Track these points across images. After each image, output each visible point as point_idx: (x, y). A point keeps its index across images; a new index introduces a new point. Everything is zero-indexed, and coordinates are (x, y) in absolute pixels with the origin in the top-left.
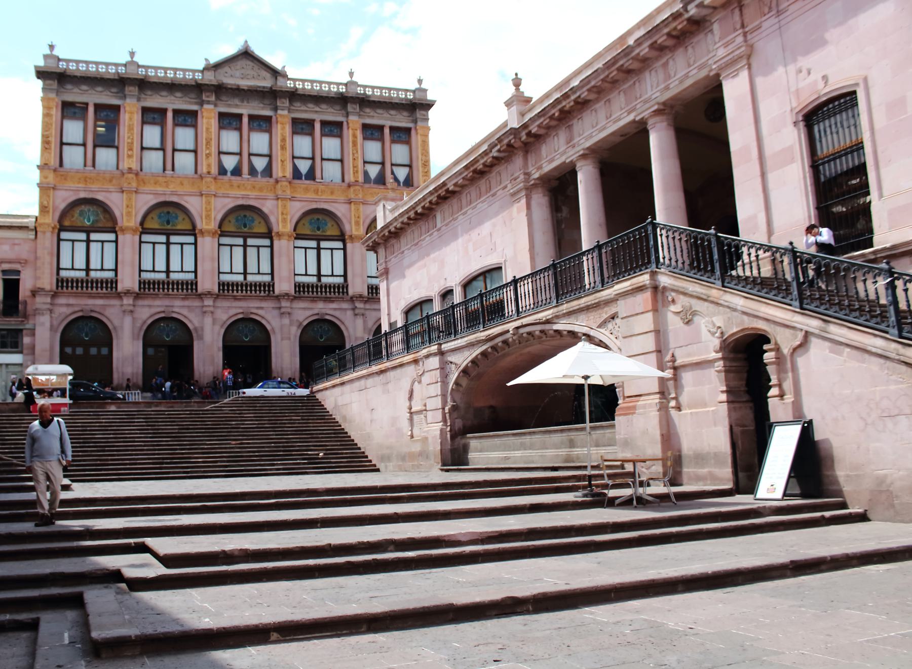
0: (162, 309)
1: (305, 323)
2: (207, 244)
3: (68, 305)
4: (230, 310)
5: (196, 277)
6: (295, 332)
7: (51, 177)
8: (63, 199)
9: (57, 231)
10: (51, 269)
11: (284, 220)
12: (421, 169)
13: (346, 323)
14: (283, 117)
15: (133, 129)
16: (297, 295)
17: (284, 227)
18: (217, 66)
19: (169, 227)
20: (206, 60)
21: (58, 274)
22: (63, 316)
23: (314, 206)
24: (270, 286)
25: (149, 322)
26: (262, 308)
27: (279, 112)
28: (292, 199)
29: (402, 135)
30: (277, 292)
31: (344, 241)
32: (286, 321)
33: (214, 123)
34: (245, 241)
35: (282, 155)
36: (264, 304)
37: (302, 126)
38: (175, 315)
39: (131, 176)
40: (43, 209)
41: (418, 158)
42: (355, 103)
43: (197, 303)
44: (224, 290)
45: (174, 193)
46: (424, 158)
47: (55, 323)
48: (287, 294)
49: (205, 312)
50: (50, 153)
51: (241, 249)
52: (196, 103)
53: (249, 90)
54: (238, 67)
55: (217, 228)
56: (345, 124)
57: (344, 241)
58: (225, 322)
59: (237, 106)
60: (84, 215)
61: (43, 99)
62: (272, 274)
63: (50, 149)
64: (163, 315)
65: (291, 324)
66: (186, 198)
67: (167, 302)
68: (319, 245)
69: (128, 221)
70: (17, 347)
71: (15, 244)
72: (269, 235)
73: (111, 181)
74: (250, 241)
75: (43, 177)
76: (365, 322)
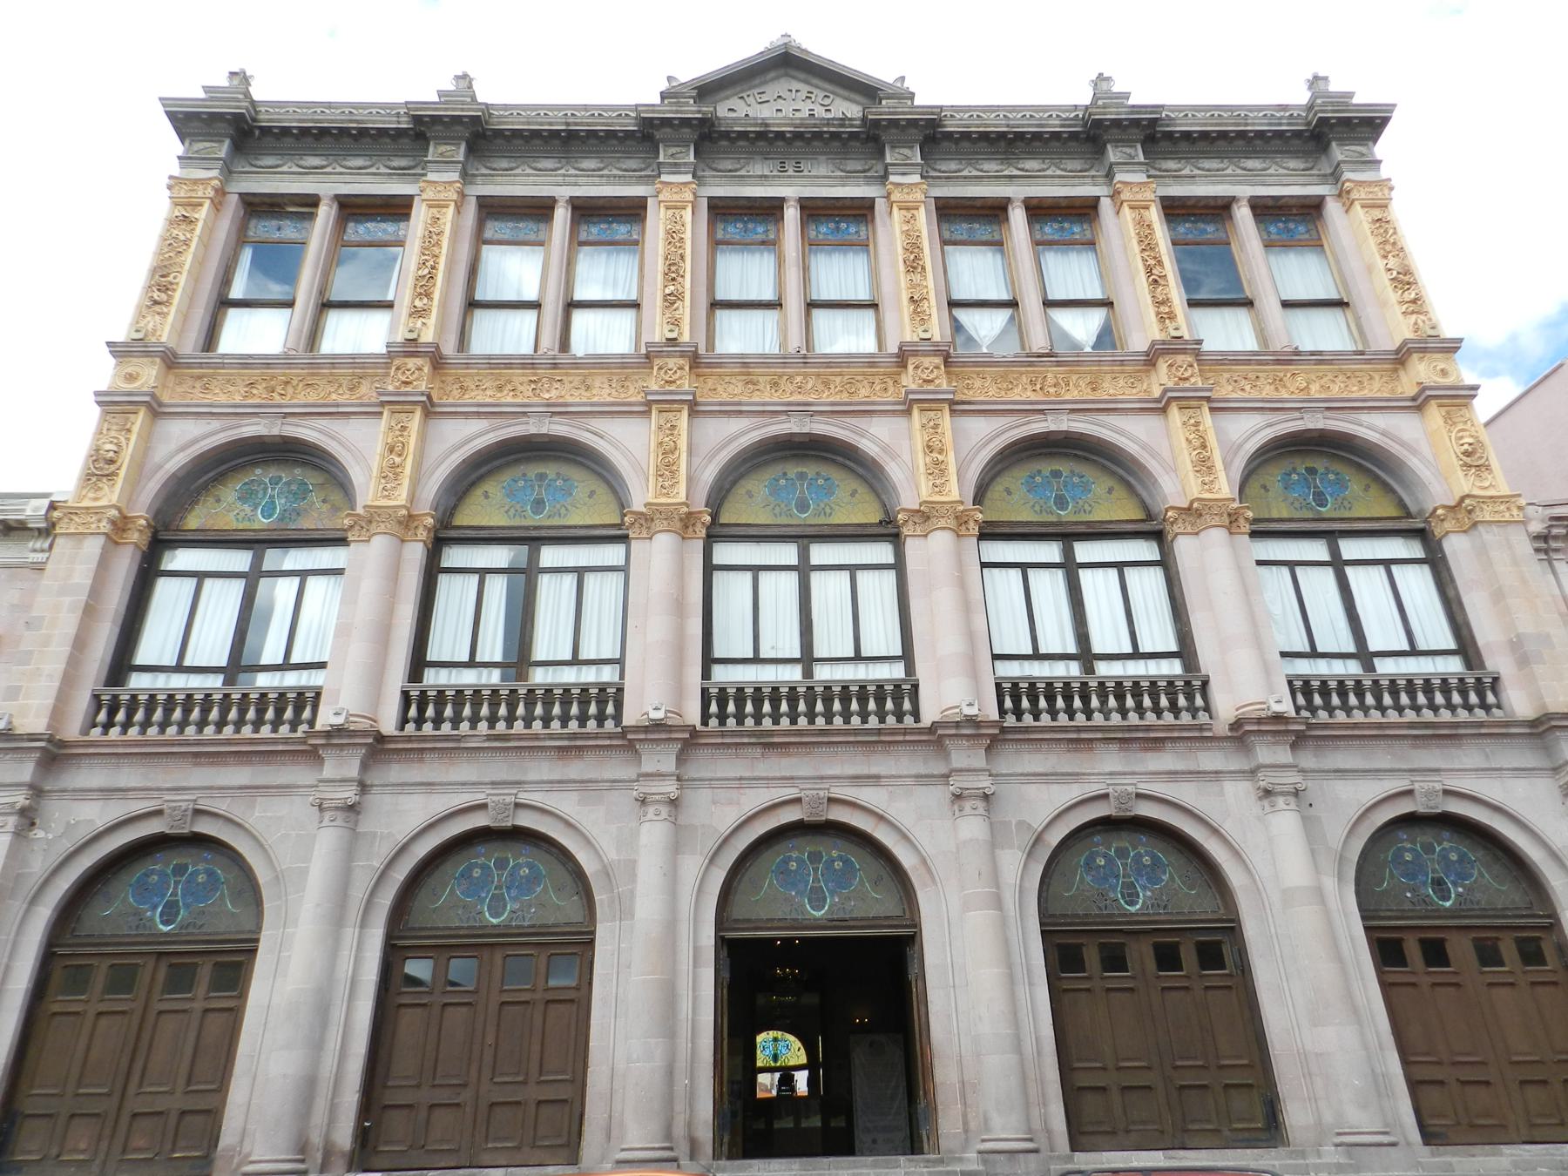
0: (477, 797)
1: (1055, 837)
3: (108, 793)
5: (622, 676)
6: (1019, 874)
7: (149, 375)
8: (183, 441)
9: (137, 537)
12: (1393, 296)
13: (1228, 828)
14: (905, 202)
15: (438, 244)
16: (1011, 720)
18: (708, 89)
20: (670, 79)
22: (83, 834)
23: (1038, 426)
24: (906, 693)
26: (874, 780)
28: (957, 407)
29: (1295, 220)
30: (929, 715)
32: (972, 827)
33: (693, 226)
34: (804, 555)
35: (913, 286)
36: (881, 764)
37: (970, 218)
38: (526, 820)
39: (412, 363)
40: (100, 468)
41: (1370, 269)
42: (1129, 142)
43: (615, 768)
44: (722, 717)
45: (558, 411)
46: (1392, 262)
47: (38, 865)
48: (971, 721)
49: (643, 802)
50: (163, 315)
51: (790, 581)
53: (798, 136)
55: (699, 505)
56: (1105, 204)
57: (1158, 536)
60: (240, 482)
61: (175, 182)
62: (907, 656)
63: (167, 303)
65: (994, 843)
66: (599, 424)
67: (499, 769)
68: (1068, 553)
72: (888, 531)
74: (821, 553)
76: (1310, 825)
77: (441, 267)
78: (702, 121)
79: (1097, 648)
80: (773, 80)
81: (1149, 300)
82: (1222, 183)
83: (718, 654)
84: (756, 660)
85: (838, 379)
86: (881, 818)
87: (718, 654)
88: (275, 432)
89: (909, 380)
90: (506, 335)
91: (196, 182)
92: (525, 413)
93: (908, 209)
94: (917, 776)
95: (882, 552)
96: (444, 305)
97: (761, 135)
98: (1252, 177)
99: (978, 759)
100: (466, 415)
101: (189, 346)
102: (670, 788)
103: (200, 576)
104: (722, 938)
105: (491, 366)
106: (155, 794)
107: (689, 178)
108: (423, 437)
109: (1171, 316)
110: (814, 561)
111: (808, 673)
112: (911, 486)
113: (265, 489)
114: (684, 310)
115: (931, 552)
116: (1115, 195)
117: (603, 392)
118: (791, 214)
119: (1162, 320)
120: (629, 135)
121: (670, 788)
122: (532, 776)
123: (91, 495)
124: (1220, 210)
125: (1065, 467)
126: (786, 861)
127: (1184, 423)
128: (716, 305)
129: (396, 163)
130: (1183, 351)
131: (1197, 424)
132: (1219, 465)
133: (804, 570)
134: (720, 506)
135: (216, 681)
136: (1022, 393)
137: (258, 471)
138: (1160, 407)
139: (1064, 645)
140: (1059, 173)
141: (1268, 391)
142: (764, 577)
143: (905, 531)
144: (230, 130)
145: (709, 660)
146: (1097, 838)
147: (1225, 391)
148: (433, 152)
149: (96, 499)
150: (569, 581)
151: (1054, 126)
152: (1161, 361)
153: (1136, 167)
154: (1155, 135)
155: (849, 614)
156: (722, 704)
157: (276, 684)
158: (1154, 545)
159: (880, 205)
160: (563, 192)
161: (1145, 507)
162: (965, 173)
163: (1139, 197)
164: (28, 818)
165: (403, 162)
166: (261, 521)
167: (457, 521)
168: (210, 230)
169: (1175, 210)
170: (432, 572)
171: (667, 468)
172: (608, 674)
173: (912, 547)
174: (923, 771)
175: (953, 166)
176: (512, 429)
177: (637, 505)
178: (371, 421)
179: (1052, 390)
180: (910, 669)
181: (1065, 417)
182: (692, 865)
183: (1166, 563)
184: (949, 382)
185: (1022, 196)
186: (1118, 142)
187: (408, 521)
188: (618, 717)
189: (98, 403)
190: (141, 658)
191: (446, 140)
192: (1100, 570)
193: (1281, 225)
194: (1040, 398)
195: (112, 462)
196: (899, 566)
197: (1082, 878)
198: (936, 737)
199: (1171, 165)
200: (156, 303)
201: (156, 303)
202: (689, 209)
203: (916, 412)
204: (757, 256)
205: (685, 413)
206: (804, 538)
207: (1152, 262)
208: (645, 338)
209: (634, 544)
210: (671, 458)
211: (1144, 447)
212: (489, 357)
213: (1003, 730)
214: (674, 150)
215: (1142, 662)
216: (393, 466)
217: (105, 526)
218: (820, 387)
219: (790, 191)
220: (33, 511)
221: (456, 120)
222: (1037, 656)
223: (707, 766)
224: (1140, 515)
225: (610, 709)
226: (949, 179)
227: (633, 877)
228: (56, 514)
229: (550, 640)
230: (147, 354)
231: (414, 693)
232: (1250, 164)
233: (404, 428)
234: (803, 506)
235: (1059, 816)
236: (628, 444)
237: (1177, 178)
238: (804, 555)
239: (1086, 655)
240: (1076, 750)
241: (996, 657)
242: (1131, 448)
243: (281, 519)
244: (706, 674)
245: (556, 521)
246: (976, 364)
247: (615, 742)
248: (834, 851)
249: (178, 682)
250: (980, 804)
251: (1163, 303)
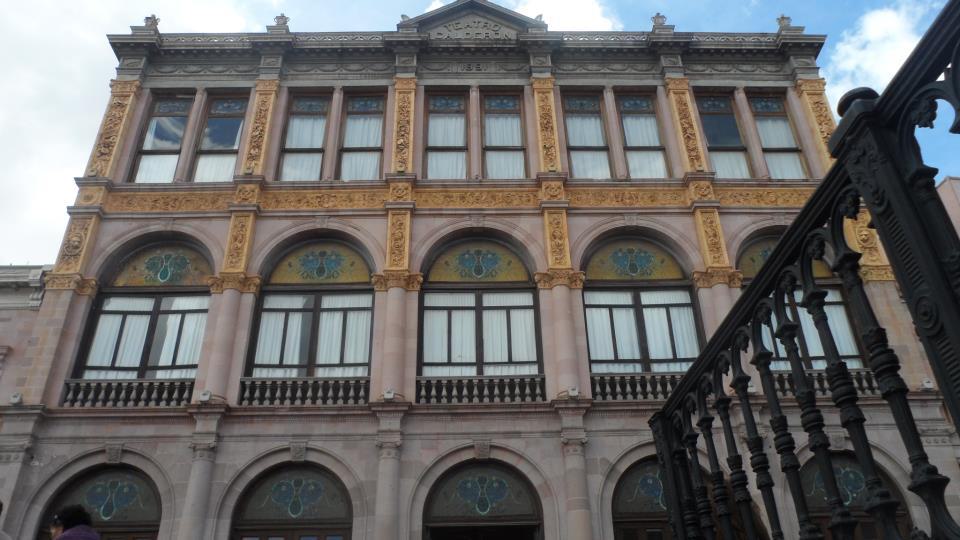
0: (285, 444)
1: (623, 467)
3: (74, 440)
4: (438, 443)
5: (369, 374)
6: (601, 488)
7: (98, 196)
8: (116, 234)
10: (55, 364)
11: (559, 249)
15: (265, 117)
16: (599, 399)
17: (559, 260)
18: (426, 22)
19: (322, 279)
20: (403, 16)
23: (619, 223)
24: (537, 384)
25: (253, 474)
26: (517, 434)
28: (571, 212)
29: (771, 102)
30: (551, 395)
31: (690, 289)
32: (574, 462)
33: (415, 103)
34: (479, 300)
35: (546, 139)
37: (580, 100)
38: (313, 458)
39: (248, 187)
40: (69, 251)
41: (812, 131)
45: (333, 214)
47: (35, 481)
48: (574, 399)
49: (380, 447)
51: (470, 316)
52: (384, 77)
53: (478, 50)
54: (459, 26)
55: (416, 269)
56: (660, 90)
57: (690, 289)
58: (429, 470)
59: (457, 75)
61: (113, 84)
62: (540, 362)
63: (109, 154)
64: (285, 458)
65: (587, 471)
66: (356, 222)
69: (233, 264)
72: (530, 286)
73: (214, 202)
74: (489, 300)
75: (84, 196)
77: (267, 130)
78: (421, 43)
79: (653, 356)
80: (464, 16)
81: (684, 147)
82: (729, 78)
83: (427, 359)
84: (449, 363)
85: (501, 194)
86: (521, 457)
87: (426, 360)
88: (169, 228)
89: (543, 195)
90: (300, 170)
91: (126, 82)
92: (314, 216)
93: (543, 93)
94: (543, 432)
95: (526, 299)
96: (267, 153)
97: (457, 50)
98: (745, 75)
99: (578, 421)
100: (280, 217)
101: (119, 179)
102: (397, 439)
103: (125, 314)
104: (427, 527)
105: (294, 188)
106: (101, 441)
107: (413, 75)
108: (254, 231)
109: (698, 158)
110: (485, 304)
111: (480, 372)
112: (543, 259)
113: (162, 262)
114: (409, 154)
115: (554, 298)
116: (665, 86)
117: (360, 202)
118: (474, 95)
119: (692, 160)
120: (378, 50)
121: (397, 439)
122: (316, 432)
123: (66, 267)
124: (728, 93)
125: (635, 247)
126: (466, 483)
127: (704, 221)
128: (428, 149)
129: (241, 68)
130: (704, 179)
131: (712, 222)
132: (724, 247)
133: (479, 309)
134: (429, 271)
135: (133, 376)
136: (610, 204)
137: (158, 252)
138: (690, 212)
139: (633, 353)
140: (634, 71)
141: (754, 203)
142: (455, 314)
143: (539, 286)
144: (143, 50)
145: (421, 364)
146: (648, 468)
147: (729, 203)
148: (264, 62)
149: (68, 269)
150: (339, 316)
151: (629, 43)
152: (691, 184)
153: (678, 70)
154: (689, 50)
155: (502, 336)
156: (428, 390)
157: (168, 377)
158: (687, 294)
159: (527, 90)
160: (339, 84)
161: (683, 272)
162: (578, 71)
163: (680, 87)
164: (30, 454)
165: (245, 68)
167: (273, 281)
168: (133, 110)
169: (700, 94)
170: (258, 311)
171: (397, 250)
172: (361, 372)
173: (543, 295)
174: (546, 428)
175: (571, 67)
176: (306, 226)
177: (379, 271)
178: (226, 222)
179: (628, 201)
180: (541, 369)
181: (635, 218)
182: (410, 483)
183: (694, 305)
184: (567, 196)
185: (611, 85)
186: (667, 55)
187: (244, 282)
188: (366, 397)
189: (70, 213)
190: (91, 362)
191: (271, 55)
192: (656, 309)
193: (763, 104)
194: (621, 205)
195: (77, 247)
196: (536, 307)
197: (638, 492)
198: (554, 409)
199: (699, 68)
200: (102, 154)
201: (102, 154)
202: (413, 94)
203: (546, 214)
204: (454, 119)
205: (408, 216)
206: (479, 290)
207: (687, 126)
208: (385, 171)
209: (377, 294)
210: (400, 243)
211: (682, 235)
212: (293, 183)
213: (593, 405)
214: (404, 59)
215: (678, 364)
216: (237, 248)
217: (73, 286)
218: (490, 199)
220: (34, 277)
221: (277, 44)
222: (617, 361)
223: (418, 427)
224: (680, 276)
225: (362, 393)
226: (568, 75)
227: (375, 491)
228: (46, 278)
229: (327, 352)
230: (97, 184)
231: (248, 383)
232: (745, 68)
233: (243, 226)
234: (479, 271)
235: (626, 454)
236: (373, 233)
237: (703, 75)
238: (479, 300)
239: (646, 360)
240: (635, 416)
241: (591, 362)
242: (674, 236)
243: (171, 280)
244: (419, 372)
245: (331, 281)
246: (583, 185)
247: (365, 412)
248: (494, 477)
249: (112, 376)
250: (579, 448)
251: (693, 150)
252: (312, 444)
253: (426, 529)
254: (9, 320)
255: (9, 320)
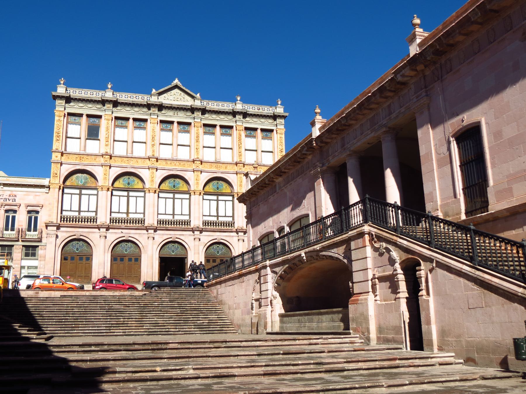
2: (151, 197)
21: (61, 213)
27: (196, 120)
34: (174, 196)
37: (209, 127)
38: (130, 239)
70: (35, 256)
71: (36, 195)
79: (219, 215)
88: (83, 168)
101: (63, 150)
155: (179, 207)
166: (80, 184)
219: (176, 120)
238: (174, 196)
252: (130, 235)
253: (159, 257)
254: (39, 196)
255: (39, 196)
